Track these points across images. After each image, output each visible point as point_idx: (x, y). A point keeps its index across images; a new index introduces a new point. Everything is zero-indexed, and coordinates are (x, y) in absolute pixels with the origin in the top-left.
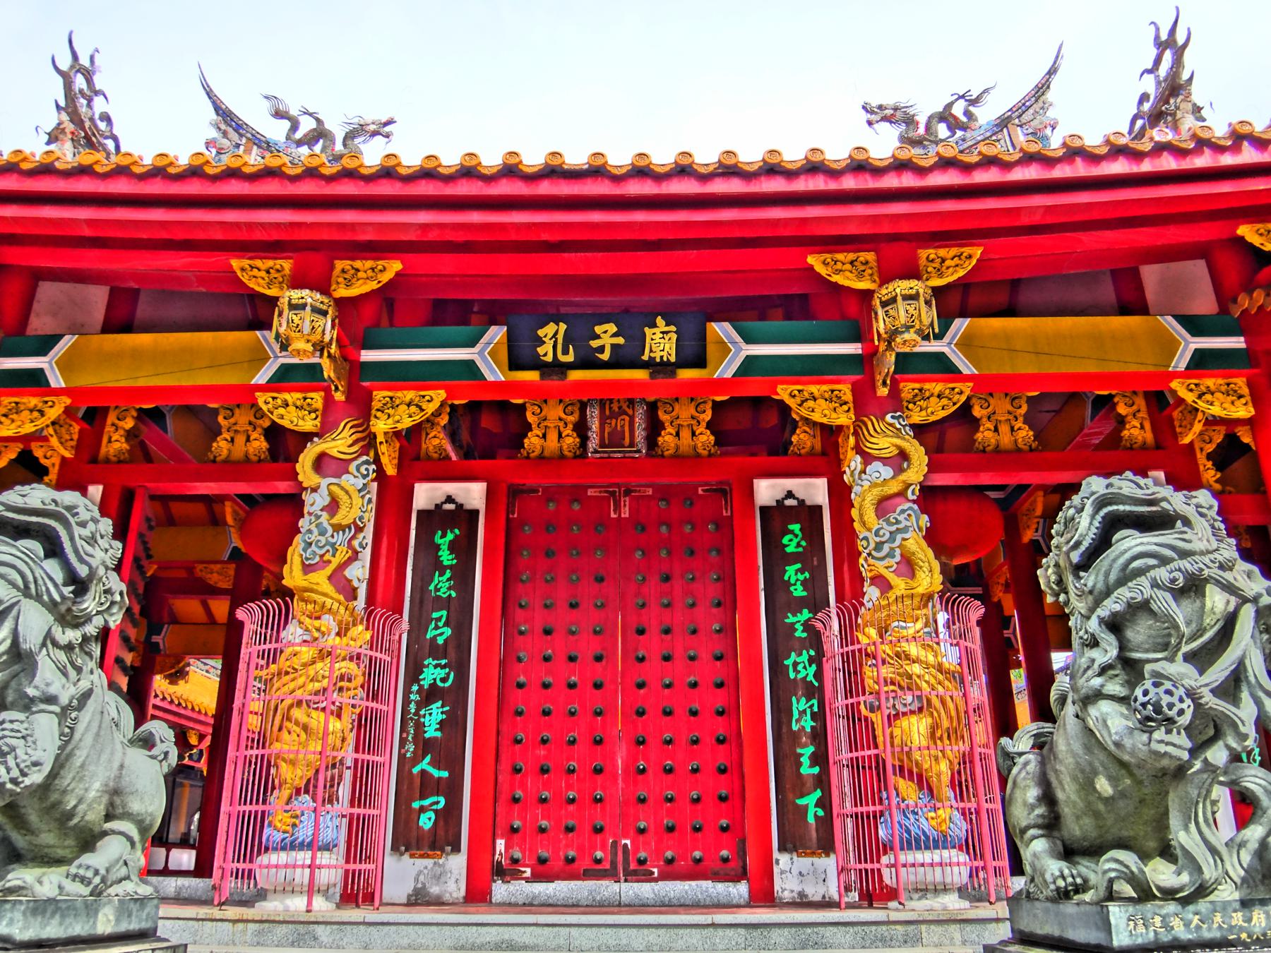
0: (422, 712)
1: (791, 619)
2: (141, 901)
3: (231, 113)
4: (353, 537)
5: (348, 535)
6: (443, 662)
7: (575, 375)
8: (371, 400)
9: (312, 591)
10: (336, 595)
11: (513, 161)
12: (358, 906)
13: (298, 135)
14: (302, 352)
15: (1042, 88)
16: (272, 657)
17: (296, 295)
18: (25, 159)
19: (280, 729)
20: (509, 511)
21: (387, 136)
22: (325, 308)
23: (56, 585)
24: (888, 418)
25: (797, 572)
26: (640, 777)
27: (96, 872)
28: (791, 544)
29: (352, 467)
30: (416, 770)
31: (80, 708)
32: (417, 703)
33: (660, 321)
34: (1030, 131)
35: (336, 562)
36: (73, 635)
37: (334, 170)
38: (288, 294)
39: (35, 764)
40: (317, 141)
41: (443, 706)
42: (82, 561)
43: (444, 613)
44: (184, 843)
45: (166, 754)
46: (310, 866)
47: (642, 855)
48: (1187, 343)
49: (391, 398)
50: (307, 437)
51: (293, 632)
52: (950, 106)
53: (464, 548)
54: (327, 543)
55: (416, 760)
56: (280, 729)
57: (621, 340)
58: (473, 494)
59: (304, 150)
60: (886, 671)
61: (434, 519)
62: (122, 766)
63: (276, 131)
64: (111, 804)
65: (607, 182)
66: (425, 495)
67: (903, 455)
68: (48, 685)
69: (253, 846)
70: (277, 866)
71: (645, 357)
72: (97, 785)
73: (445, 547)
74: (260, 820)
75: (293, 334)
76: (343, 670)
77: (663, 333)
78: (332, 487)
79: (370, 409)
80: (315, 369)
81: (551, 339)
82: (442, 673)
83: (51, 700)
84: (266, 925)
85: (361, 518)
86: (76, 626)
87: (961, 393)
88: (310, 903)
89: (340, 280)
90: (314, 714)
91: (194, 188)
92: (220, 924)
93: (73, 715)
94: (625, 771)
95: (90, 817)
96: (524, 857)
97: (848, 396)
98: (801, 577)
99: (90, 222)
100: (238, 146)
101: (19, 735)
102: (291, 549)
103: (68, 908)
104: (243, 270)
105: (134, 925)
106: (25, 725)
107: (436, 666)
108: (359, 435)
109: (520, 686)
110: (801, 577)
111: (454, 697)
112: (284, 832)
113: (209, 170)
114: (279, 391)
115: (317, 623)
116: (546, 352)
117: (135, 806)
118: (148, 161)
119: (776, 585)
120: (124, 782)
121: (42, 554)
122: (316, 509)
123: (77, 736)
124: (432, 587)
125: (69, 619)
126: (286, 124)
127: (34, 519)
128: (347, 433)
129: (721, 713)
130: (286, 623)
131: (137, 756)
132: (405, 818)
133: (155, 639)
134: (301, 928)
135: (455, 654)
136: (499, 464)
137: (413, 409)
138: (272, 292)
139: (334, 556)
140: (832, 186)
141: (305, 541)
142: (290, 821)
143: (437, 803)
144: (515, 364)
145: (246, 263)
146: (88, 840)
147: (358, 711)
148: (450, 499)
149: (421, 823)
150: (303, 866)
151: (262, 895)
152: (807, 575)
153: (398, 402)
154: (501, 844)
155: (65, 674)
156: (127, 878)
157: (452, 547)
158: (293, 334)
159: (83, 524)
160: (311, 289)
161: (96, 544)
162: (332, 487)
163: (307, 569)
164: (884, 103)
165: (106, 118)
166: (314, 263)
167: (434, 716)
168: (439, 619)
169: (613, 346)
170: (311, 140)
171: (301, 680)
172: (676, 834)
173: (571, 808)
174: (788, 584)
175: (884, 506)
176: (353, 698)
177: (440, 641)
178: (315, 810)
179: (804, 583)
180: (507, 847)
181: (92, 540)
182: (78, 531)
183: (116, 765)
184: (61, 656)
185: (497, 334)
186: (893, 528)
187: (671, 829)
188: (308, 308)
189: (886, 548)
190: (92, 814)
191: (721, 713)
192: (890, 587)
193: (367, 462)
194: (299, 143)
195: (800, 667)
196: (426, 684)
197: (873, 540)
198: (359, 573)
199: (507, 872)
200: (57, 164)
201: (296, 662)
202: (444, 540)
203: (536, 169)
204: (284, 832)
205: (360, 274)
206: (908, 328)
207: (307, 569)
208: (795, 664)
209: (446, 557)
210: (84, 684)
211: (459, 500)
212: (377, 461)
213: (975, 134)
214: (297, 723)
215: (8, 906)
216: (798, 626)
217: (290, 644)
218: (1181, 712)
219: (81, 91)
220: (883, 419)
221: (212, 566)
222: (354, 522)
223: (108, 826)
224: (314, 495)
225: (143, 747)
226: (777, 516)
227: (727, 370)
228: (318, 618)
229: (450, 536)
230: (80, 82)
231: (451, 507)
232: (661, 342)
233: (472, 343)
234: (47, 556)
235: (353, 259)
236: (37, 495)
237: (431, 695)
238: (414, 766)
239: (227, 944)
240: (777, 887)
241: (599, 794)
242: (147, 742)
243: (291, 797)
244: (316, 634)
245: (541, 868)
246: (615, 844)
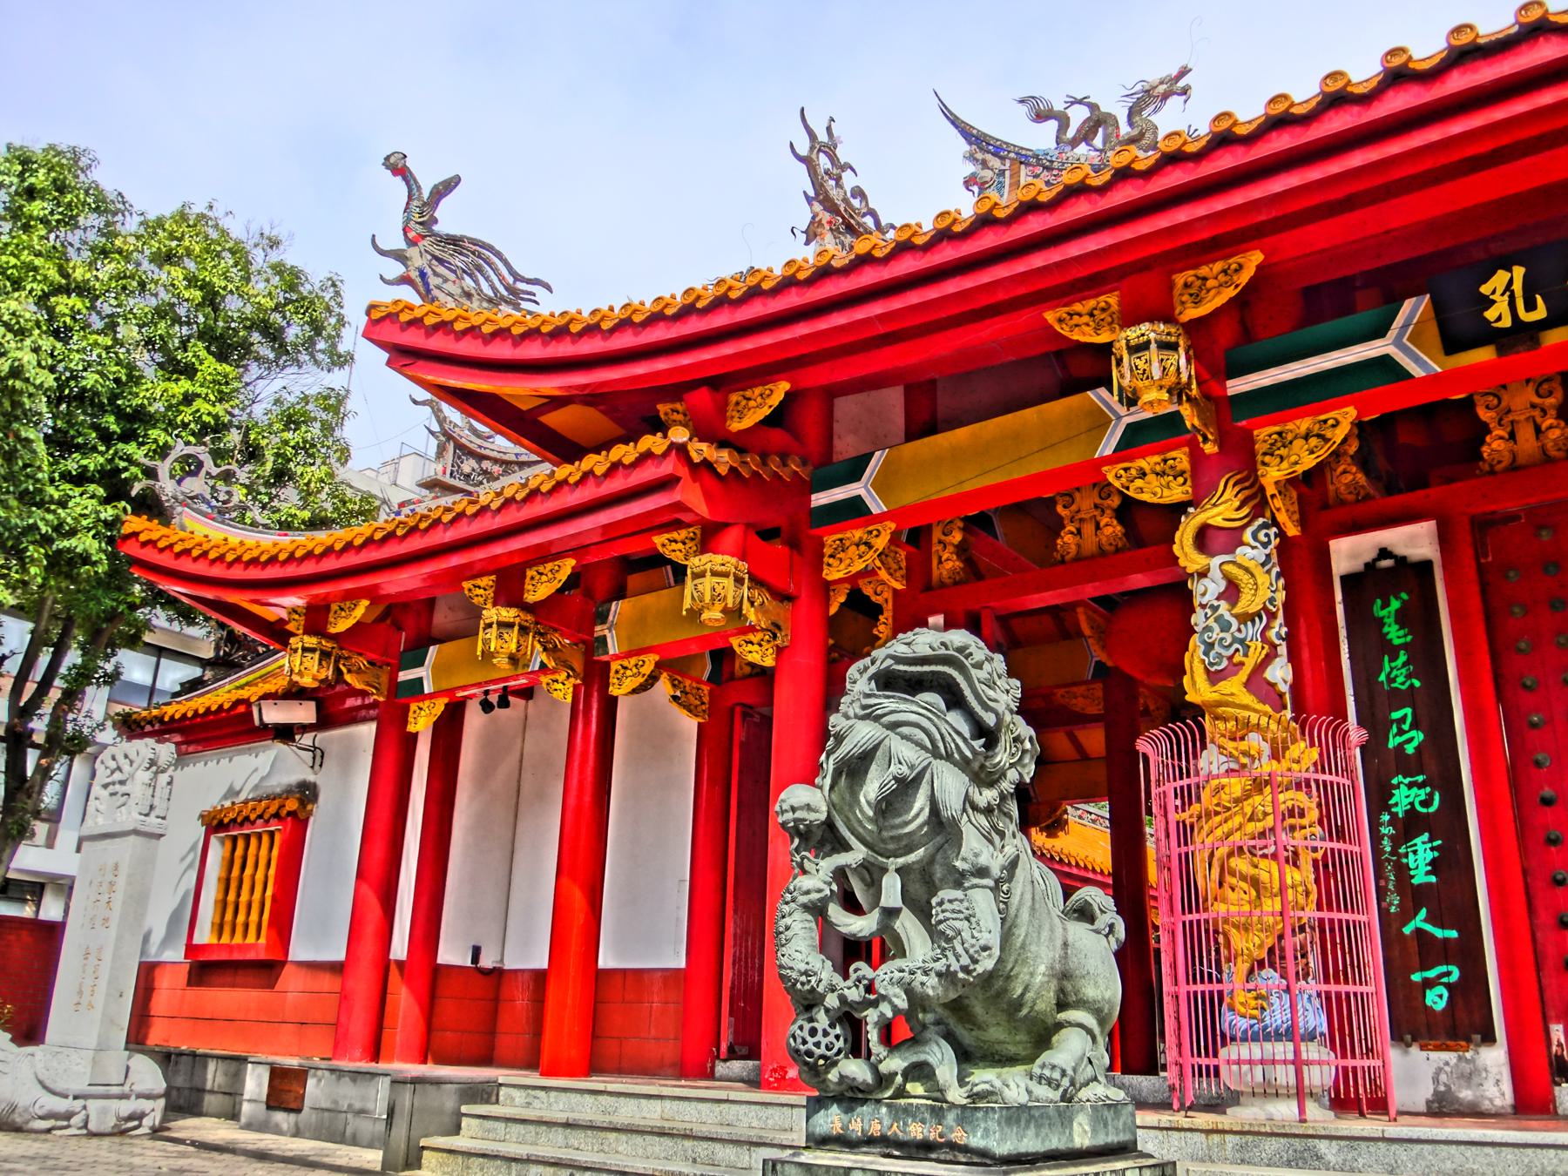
0: (1402, 850)
2: (1114, 1107)
4: (1267, 627)
5: (1260, 626)
6: (1420, 778)
9: (1227, 704)
10: (1260, 706)
11: (1397, 61)
12: (1362, 1115)
13: (1071, 133)
14: (1155, 402)
16: (1187, 797)
17: (1133, 334)
18: (800, 269)
19: (1221, 884)
20: (1479, 550)
21: (1185, 91)
22: (1173, 339)
23: (965, 740)
29: (1247, 536)
30: (1407, 930)
31: (1011, 878)
32: (1391, 838)
36: (988, 796)
37: (1151, 162)
38: (1123, 335)
39: (985, 948)
41: (1431, 840)
42: (987, 708)
43: (1408, 711)
45: (1111, 926)
46: (1293, 1062)
49: (1280, 434)
50: (1179, 509)
51: (1210, 761)
53: (1420, 617)
54: (1235, 640)
55: (1407, 915)
56: (1221, 884)
58: (1415, 540)
59: (1082, 149)
62: (1065, 945)
63: (1041, 138)
65: (1554, 39)
66: (1348, 553)
68: (976, 855)
69: (1212, 1038)
70: (1250, 1062)
72: (1042, 968)
74: (1213, 1004)
75: (1140, 384)
76: (1290, 804)
78: (1225, 567)
79: (1253, 454)
80: (1176, 418)
82: (1422, 794)
83: (982, 872)
84: (1250, 1138)
85: (1272, 600)
86: (991, 784)
88: (1302, 1110)
89: (1184, 298)
90: (1264, 863)
91: (989, 240)
92: (1189, 1134)
93: (1005, 888)
95: (1041, 1006)
99: (881, 318)
100: (1002, 173)
102: (1187, 655)
103: (1042, 1116)
104: (1060, 321)
105: (1112, 1138)
106: (966, 904)
107: (1410, 786)
108: (1247, 493)
109: (1546, 802)
111: (1448, 827)
112: (1253, 1017)
113: (1000, 214)
114: (1131, 459)
115: (1243, 745)
116: (1498, 314)
117: (1090, 992)
118: (928, 226)
120: (1073, 963)
121: (943, 706)
123: (1012, 911)
124: (1382, 678)
125: (984, 777)
126: (1053, 125)
127: (926, 668)
130: (1204, 747)
131: (1078, 931)
134: (1297, 1142)
137: (1313, 441)
138: (1103, 338)
139: (1246, 655)
141: (1204, 642)
142: (1253, 1003)
143: (1448, 974)
144: (1452, 345)
145: (1062, 312)
146: (1043, 1036)
147: (1319, 855)
148: (1384, 553)
149: (1428, 1002)
150: (1285, 1062)
151: (1234, 1098)
153: (1290, 436)
155: (991, 842)
156: (1095, 1079)
157: (1402, 618)
158: (1140, 384)
159: (979, 666)
160: (1151, 321)
161: (997, 688)
162: (1225, 567)
163: (1214, 677)
165: (859, 193)
166: (1143, 286)
167: (1421, 856)
170: (1086, 135)
171: (1238, 820)
176: (1310, 838)
178: (1288, 990)
181: (991, 684)
182: (974, 672)
183: (1059, 943)
184: (982, 820)
185: (1413, 309)
188: (1153, 346)
190: (1044, 1002)
193: (1264, 526)
194: (1074, 143)
196: (1400, 811)
198: (1280, 673)
200: (833, 263)
201: (1225, 798)
202: (1388, 611)
203: (1436, 60)
204: (1253, 1017)
205: (1210, 283)
207: (1214, 677)
209: (1395, 634)
210: (1010, 850)
212: (1275, 523)
214: (1243, 878)
215: (980, 1114)
217: (1210, 777)
219: (827, 172)
221: (1075, 689)
222: (1265, 608)
223: (1062, 1016)
224: (1205, 581)
225: (1078, 919)
228: (1242, 739)
229: (1395, 604)
230: (824, 162)
231: (1387, 563)
233: (1379, 332)
234: (948, 709)
235: (1196, 266)
236: (924, 641)
237: (1410, 825)
238: (1405, 923)
239: (1203, 1161)
242: (1085, 914)
243: (1251, 971)
244: (1245, 760)
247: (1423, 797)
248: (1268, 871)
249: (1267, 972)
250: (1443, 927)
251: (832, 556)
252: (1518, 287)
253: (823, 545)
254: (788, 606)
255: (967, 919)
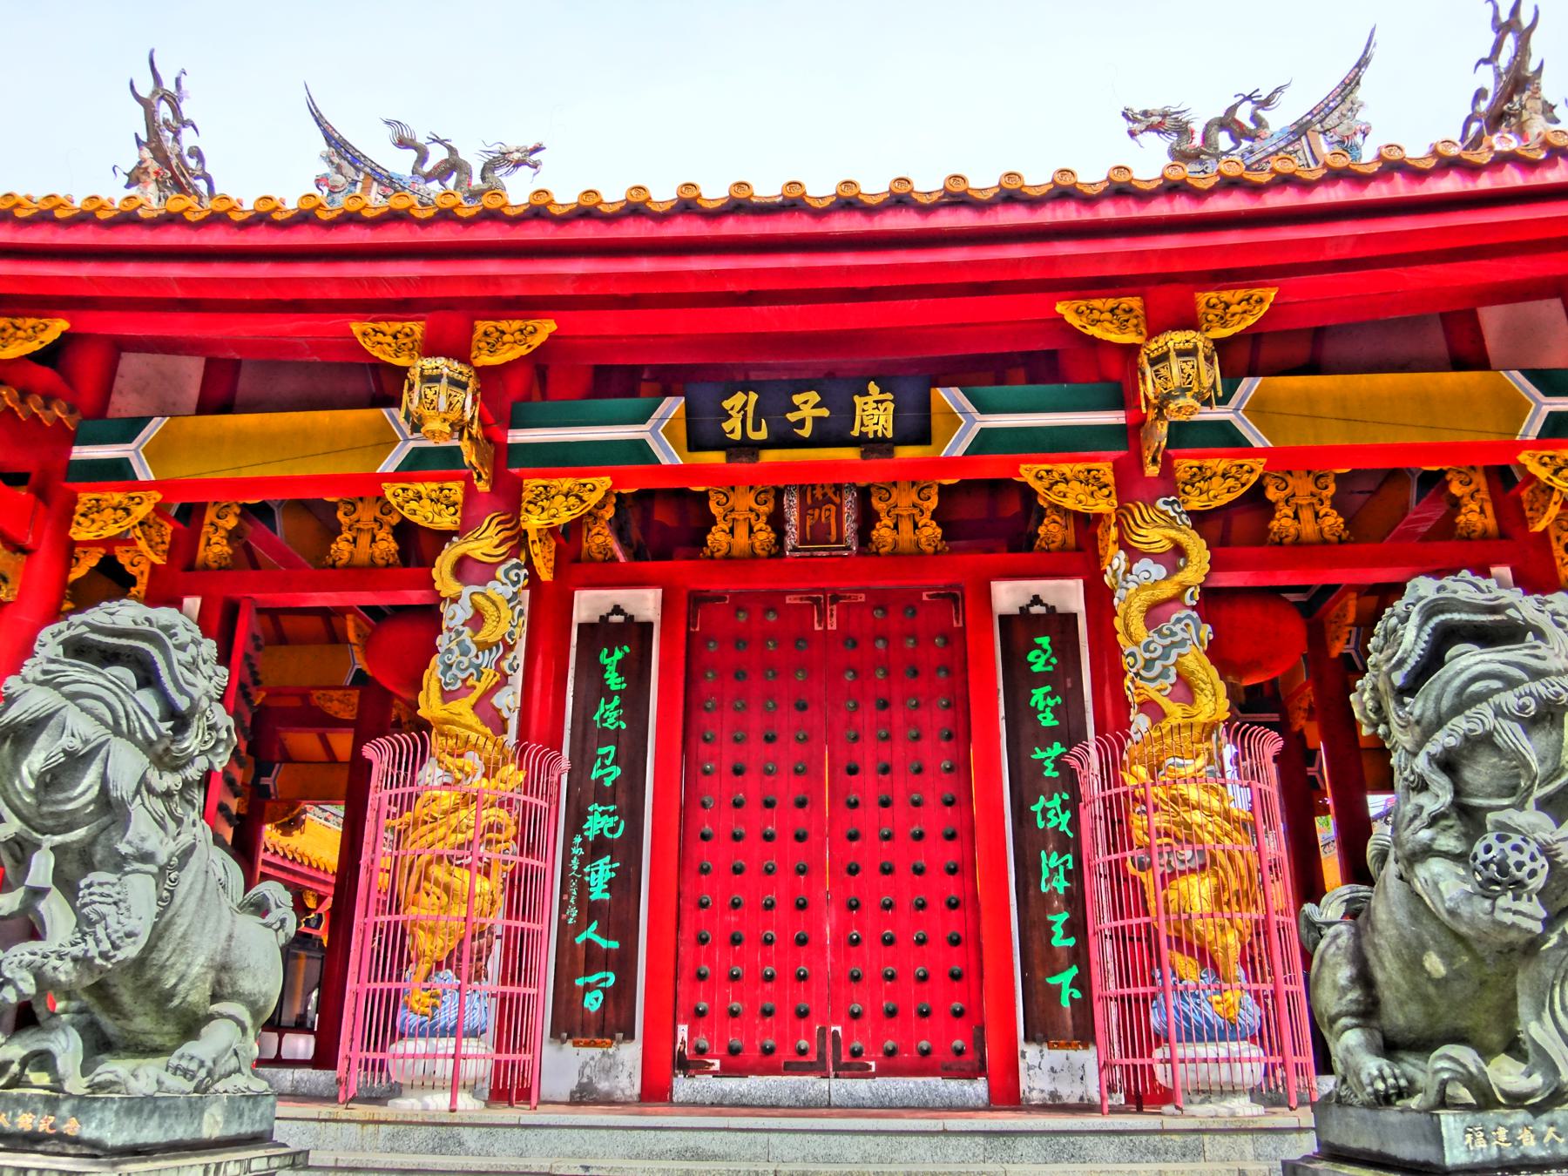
0: (587, 870)
1: (1039, 754)
2: (255, 1098)
3: (346, 142)
4: (502, 657)
5: (496, 655)
6: (612, 808)
7: (769, 456)
8: (520, 489)
9: (453, 723)
10: (482, 728)
11: (690, 194)
12: (511, 1105)
13: (427, 168)
14: (437, 433)
15: (1350, 84)
16: (406, 803)
17: (429, 364)
18: (102, 207)
19: (418, 889)
21: (535, 166)
22: (464, 379)
23: (151, 720)
24: (1160, 504)
25: (1046, 696)
26: (854, 950)
27: (202, 1064)
28: (1039, 661)
29: (500, 573)
30: (579, 940)
31: (180, 868)
32: (580, 858)
33: (873, 388)
34: (1336, 138)
35: (481, 687)
36: (172, 781)
37: (472, 212)
38: (419, 363)
39: (129, 935)
40: (450, 175)
42: (182, 691)
43: (612, 749)
44: (300, 1026)
45: (283, 921)
46: (453, 1056)
47: (857, 1045)
48: (1539, 404)
49: (545, 487)
50: (445, 536)
51: (431, 773)
52: (1233, 109)
53: (635, 670)
54: (471, 665)
55: (580, 927)
56: (418, 889)
57: (825, 412)
58: (645, 603)
59: (435, 186)
60: (1158, 820)
61: (599, 634)
62: (230, 937)
63: (400, 163)
64: (218, 982)
65: (806, 218)
66: (588, 605)
67: (1179, 550)
68: (143, 839)
69: (386, 1030)
70: (414, 1056)
71: (855, 433)
72: (201, 960)
73: (611, 668)
74: (393, 1001)
75: (426, 412)
76: (492, 819)
77: (877, 402)
78: (475, 597)
80: (453, 454)
81: (739, 412)
82: (609, 822)
83: (146, 857)
84: (402, 1127)
85: (511, 634)
86: (175, 769)
87: (1252, 471)
88: (453, 1100)
89: (482, 345)
90: (457, 872)
91: (304, 237)
92: (346, 1125)
93: (173, 876)
94: (835, 941)
95: (194, 997)
96: (712, 1046)
97: (1110, 478)
98: (1051, 702)
99: (182, 281)
100: (354, 183)
101: (110, 900)
102: (427, 672)
103: (169, 1107)
104: (365, 334)
105: (246, 1128)
106: (117, 888)
107: (603, 813)
109: (704, 837)
110: (1051, 702)
111: (625, 850)
112: (423, 1015)
113: (323, 215)
114: (410, 480)
115: (459, 762)
117: (246, 984)
118: (248, 206)
119: (1020, 712)
120: (235, 954)
121: (134, 683)
122: (457, 623)
123: (178, 900)
124: (597, 717)
125: (166, 760)
126: (412, 155)
128: (492, 530)
129: (952, 872)
130: (423, 761)
131: (249, 924)
132: (566, 999)
133: (265, 781)
134: (443, 1131)
135: (626, 796)
136: (678, 567)
137: (572, 500)
138: (401, 361)
139: (479, 680)
140: (1087, 215)
141: (444, 663)
142: (428, 1001)
143: (606, 979)
144: (695, 444)
145: (368, 326)
146: (191, 1025)
147: (510, 868)
148: (617, 610)
149: (586, 1005)
150: (445, 1056)
151: (396, 1091)
152: (1059, 699)
153: (553, 492)
154: (683, 1031)
155: (163, 827)
156: (239, 1070)
157: (621, 668)
158: (426, 412)
159: (182, 647)
160: (447, 357)
161: (199, 673)
162: (475, 597)
163: (447, 696)
164: (1150, 108)
165: (197, 153)
167: (600, 875)
168: (606, 756)
169: (816, 420)
170: (442, 173)
171: (441, 832)
172: (897, 1020)
173: (769, 987)
174: (1035, 711)
175: (1155, 614)
176: (507, 853)
177: (608, 782)
178: (459, 989)
179: (1055, 710)
180: (691, 1034)
181: (193, 666)
182: (176, 655)
183: (224, 935)
184: (159, 805)
185: (673, 406)
186: (1167, 641)
187: (891, 1014)
188: (444, 380)
189: (1158, 666)
190: (196, 995)
191: (952, 872)
192: (1164, 715)
193: (517, 566)
194: (428, 178)
195: (1050, 815)
196: (591, 835)
197: (1142, 656)
198: (508, 700)
199: (690, 1065)
200: (140, 212)
201: (435, 810)
202: (611, 660)
203: (718, 204)
204: (423, 1015)
205: (507, 338)
206: (1184, 391)
207: (447, 696)
208: (1045, 810)
209: (614, 681)
210: (185, 839)
211: (629, 611)
212: (529, 564)
213: (1266, 144)
214: (437, 883)
215: (98, 1105)
216: (1048, 763)
217: (427, 787)
218: (1533, 874)
219: (166, 122)
220: (1153, 505)
221: (332, 693)
222: (503, 640)
224: (454, 606)
225: (253, 913)
226: (1020, 627)
227: (956, 446)
228: (461, 756)
229: (618, 655)
230: (164, 111)
232: (875, 413)
233: (643, 420)
234: (140, 686)
235: (497, 319)
236: (126, 613)
237: (597, 848)
238: (577, 935)
239: (355, 1150)
240: (1023, 1086)
241: (803, 969)
242: (260, 908)
243: (430, 973)
244: (459, 776)
245: (732, 1060)
246: (823, 1031)
247: (611, 825)
250: (608, 939)
251: (83, 515)
252: (750, 409)
253: (75, 501)
254: (21, 558)
255: (115, 903)
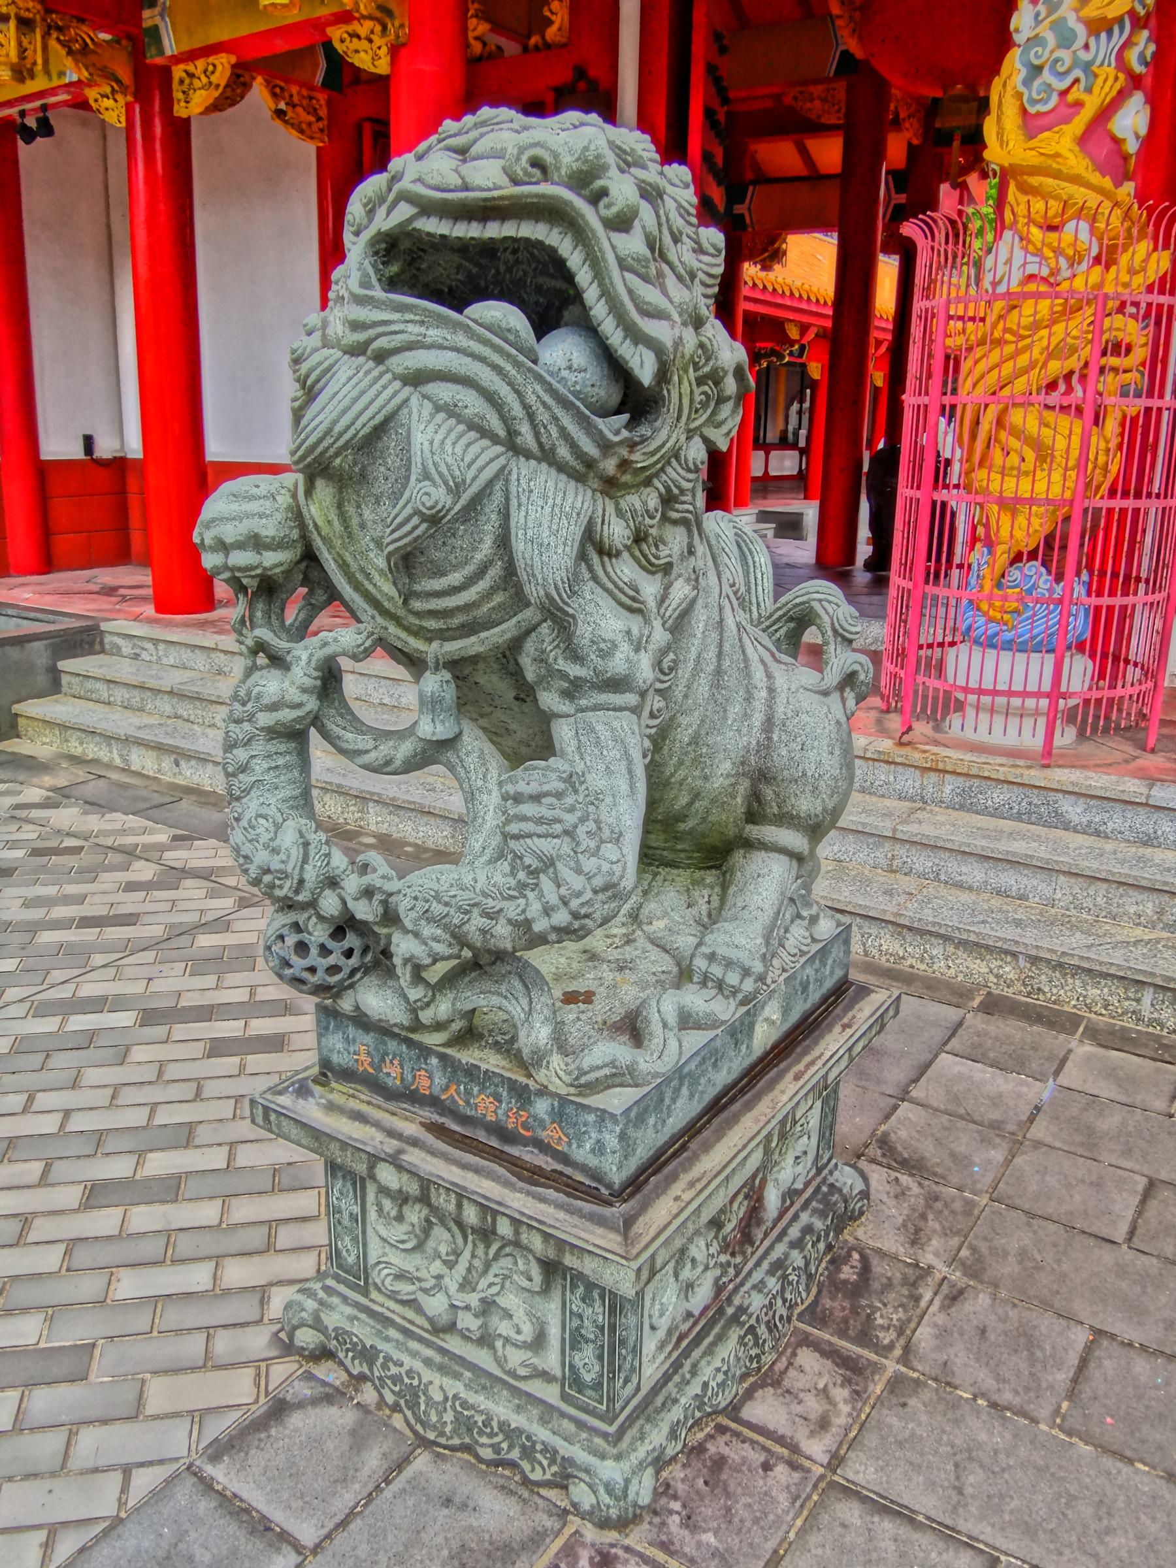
5: (1118, 40)
10: (1095, 178)
27: (746, 972)
35: (1092, 105)
44: (785, 443)
46: (1047, 695)
54: (1076, 63)
62: (769, 724)
64: (756, 796)
101: (558, 828)
102: (997, 83)
127: (494, 230)
131: (795, 681)
133: (739, 209)
139: (1089, 90)
163: (1032, 125)
183: (758, 719)
198: (1132, 121)
207: (1032, 125)
221: (812, 89)
223: (753, 831)
248: (1064, 435)
249: (1033, 568)
255: (566, 832)
